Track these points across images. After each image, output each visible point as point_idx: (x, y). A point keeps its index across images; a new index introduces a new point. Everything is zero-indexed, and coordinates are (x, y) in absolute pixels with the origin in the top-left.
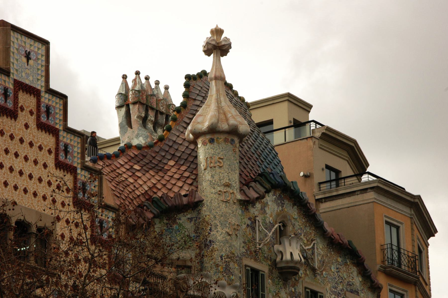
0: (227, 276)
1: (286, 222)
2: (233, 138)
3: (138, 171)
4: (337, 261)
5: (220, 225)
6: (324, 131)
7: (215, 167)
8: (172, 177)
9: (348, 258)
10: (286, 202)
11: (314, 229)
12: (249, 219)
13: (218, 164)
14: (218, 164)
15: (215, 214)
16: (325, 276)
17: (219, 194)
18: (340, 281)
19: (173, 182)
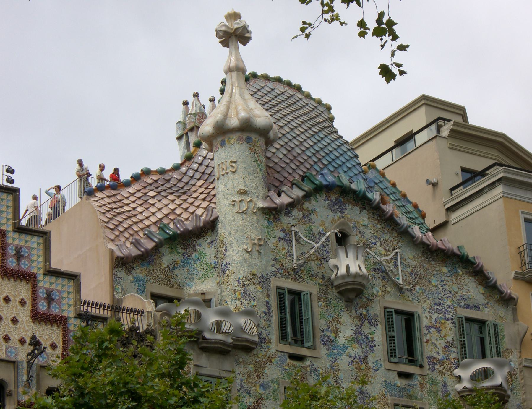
0: (246, 302)
1: (348, 230)
2: (249, 135)
3: (153, 197)
4: (441, 272)
5: (235, 243)
6: (452, 127)
7: (227, 173)
8: (196, 198)
9: (459, 267)
10: (349, 207)
11: (396, 235)
12: (281, 231)
13: (231, 169)
14: (231, 169)
15: (230, 230)
16: (421, 292)
17: (234, 205)
18: (448, 295)
19: (197, 203)
